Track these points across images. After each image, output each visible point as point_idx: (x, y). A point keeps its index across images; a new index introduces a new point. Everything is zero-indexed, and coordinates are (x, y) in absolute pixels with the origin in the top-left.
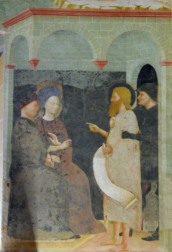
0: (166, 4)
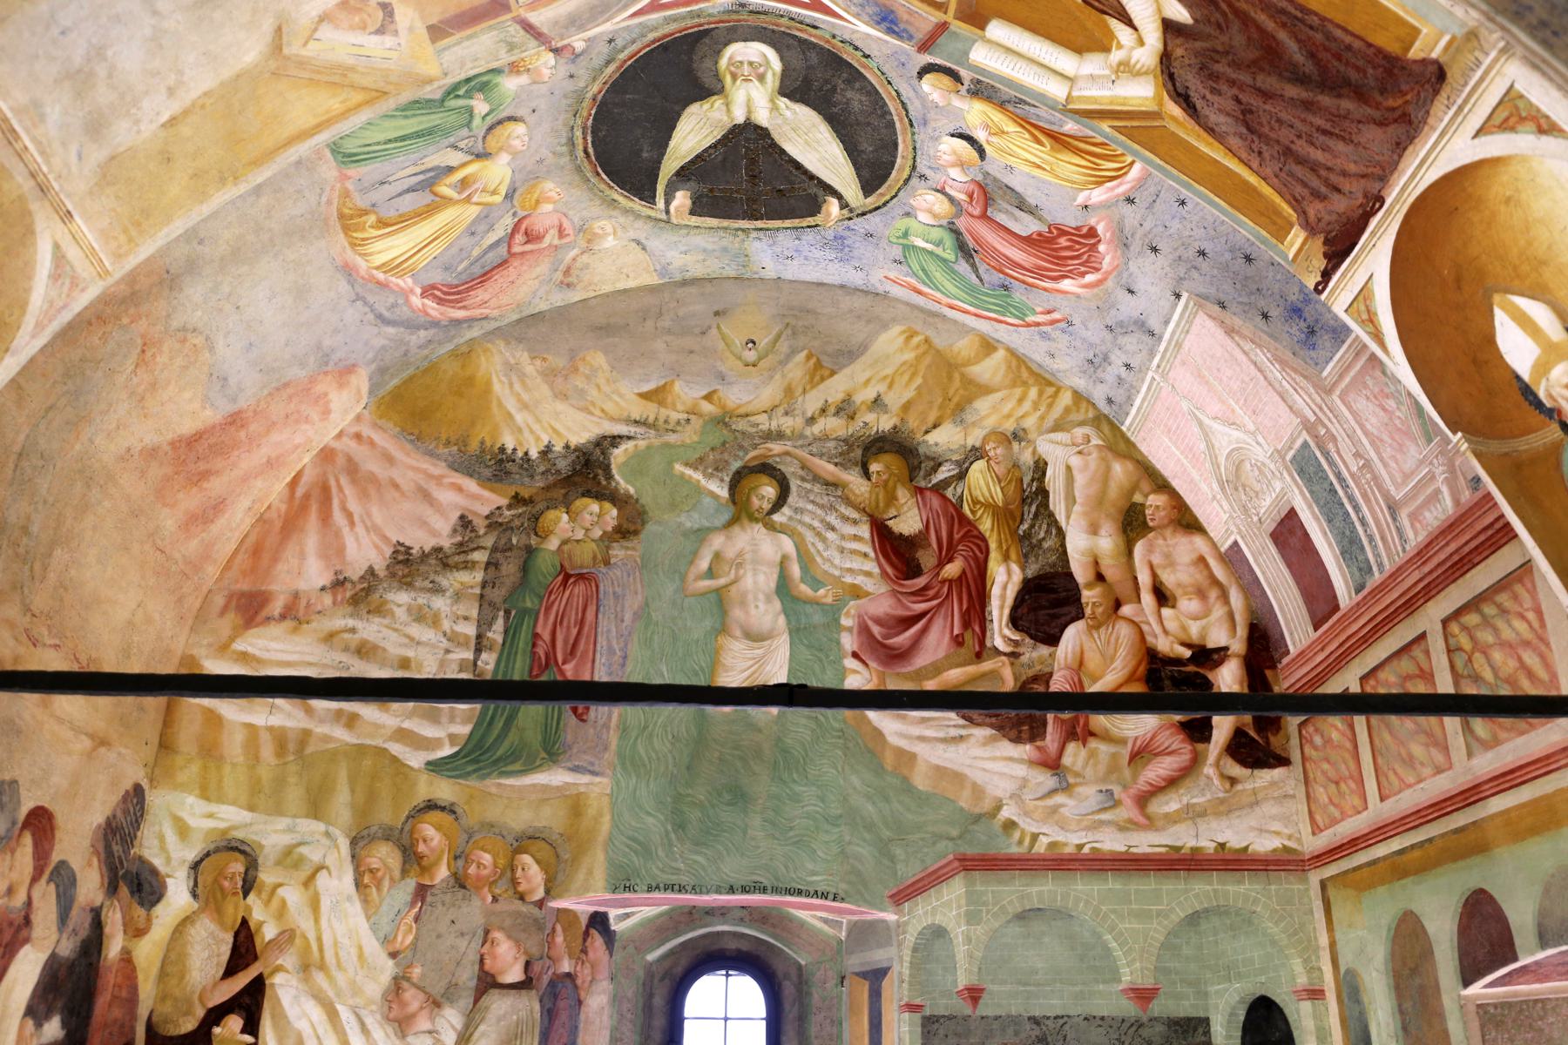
0: (1290, 837)
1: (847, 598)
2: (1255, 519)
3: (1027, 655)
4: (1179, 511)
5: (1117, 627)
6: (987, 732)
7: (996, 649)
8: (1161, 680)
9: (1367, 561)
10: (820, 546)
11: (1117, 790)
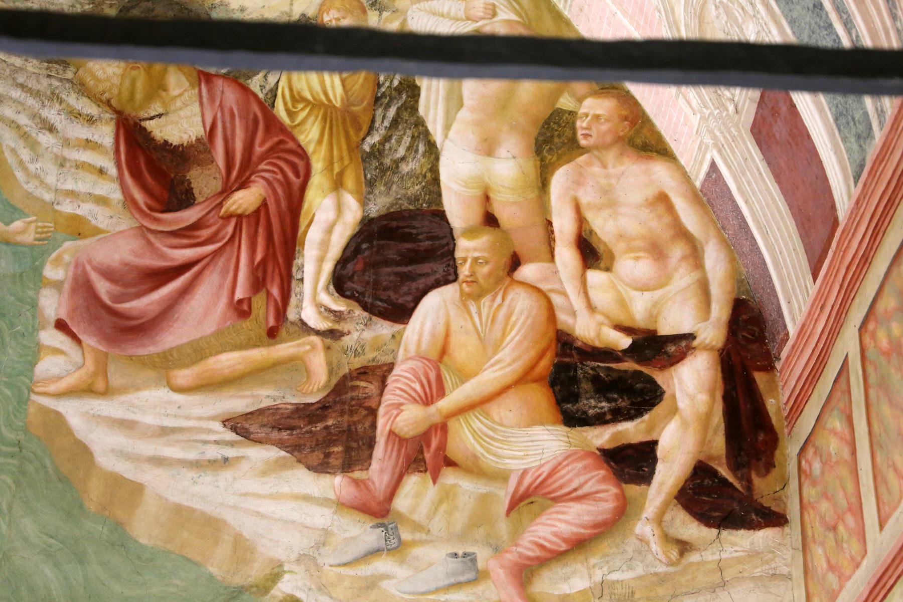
1: (60, 236)
2: (731, 108)
3: (355, 335)
4: (633, 123)
5: (510, 297)
6: (273, 453)
7: (303, 323)
8: (575, 380)
9: (866, 114)
10: (25, 154)
11: (483, 555)
